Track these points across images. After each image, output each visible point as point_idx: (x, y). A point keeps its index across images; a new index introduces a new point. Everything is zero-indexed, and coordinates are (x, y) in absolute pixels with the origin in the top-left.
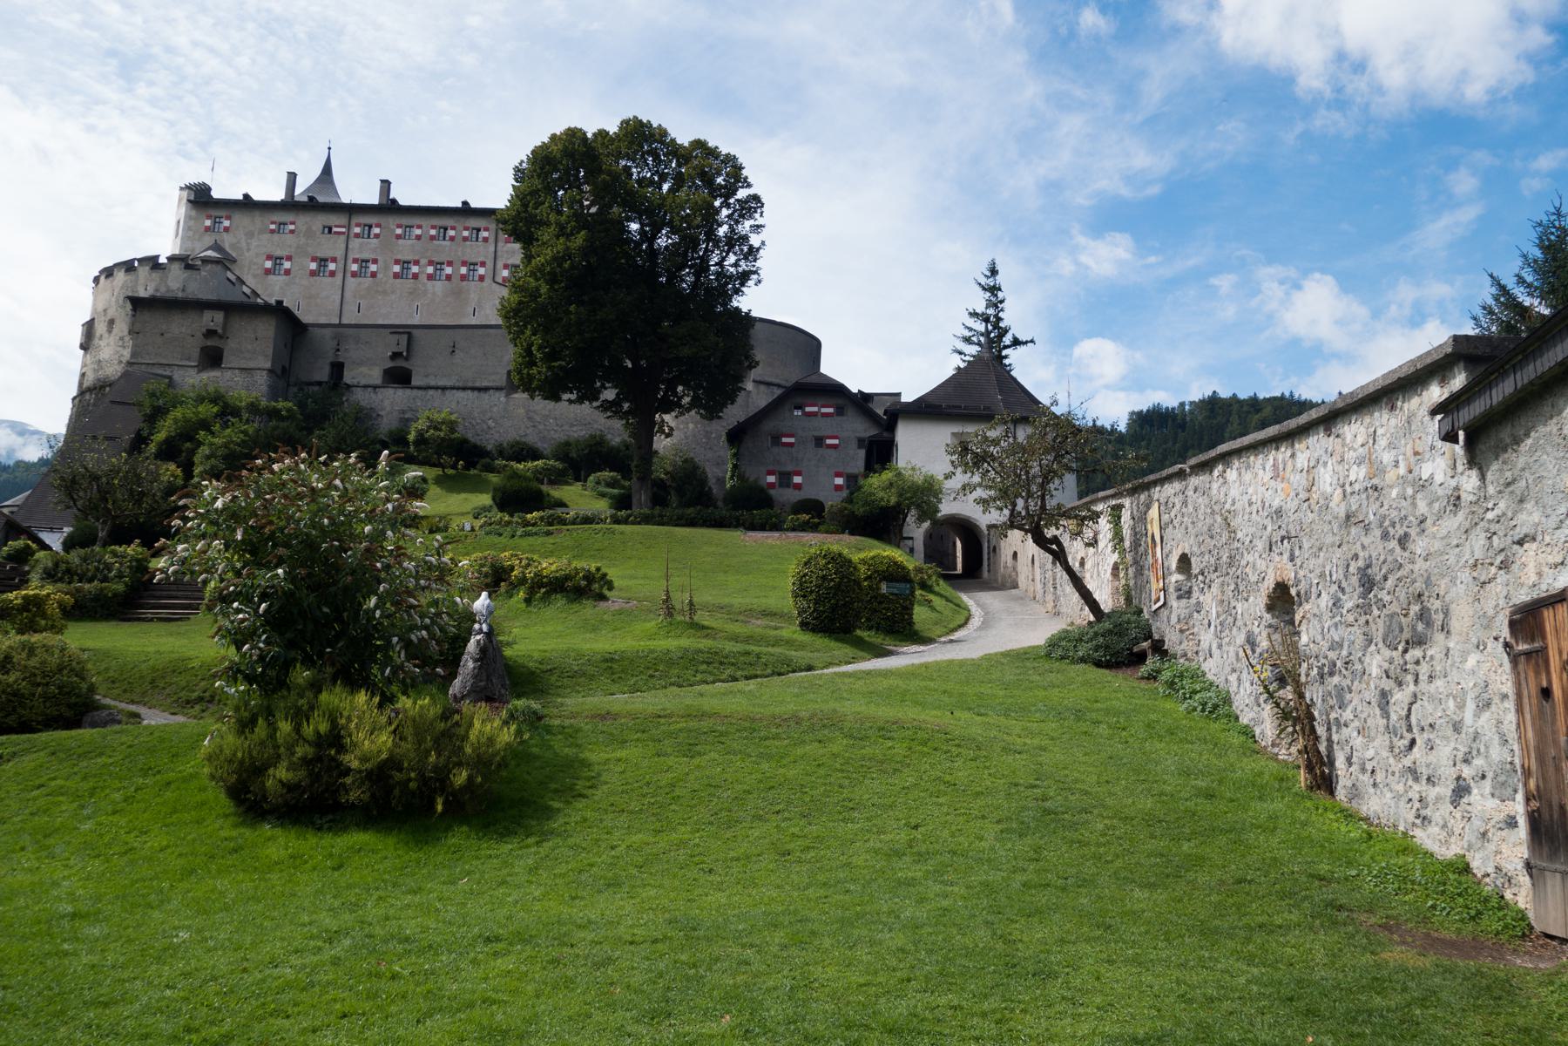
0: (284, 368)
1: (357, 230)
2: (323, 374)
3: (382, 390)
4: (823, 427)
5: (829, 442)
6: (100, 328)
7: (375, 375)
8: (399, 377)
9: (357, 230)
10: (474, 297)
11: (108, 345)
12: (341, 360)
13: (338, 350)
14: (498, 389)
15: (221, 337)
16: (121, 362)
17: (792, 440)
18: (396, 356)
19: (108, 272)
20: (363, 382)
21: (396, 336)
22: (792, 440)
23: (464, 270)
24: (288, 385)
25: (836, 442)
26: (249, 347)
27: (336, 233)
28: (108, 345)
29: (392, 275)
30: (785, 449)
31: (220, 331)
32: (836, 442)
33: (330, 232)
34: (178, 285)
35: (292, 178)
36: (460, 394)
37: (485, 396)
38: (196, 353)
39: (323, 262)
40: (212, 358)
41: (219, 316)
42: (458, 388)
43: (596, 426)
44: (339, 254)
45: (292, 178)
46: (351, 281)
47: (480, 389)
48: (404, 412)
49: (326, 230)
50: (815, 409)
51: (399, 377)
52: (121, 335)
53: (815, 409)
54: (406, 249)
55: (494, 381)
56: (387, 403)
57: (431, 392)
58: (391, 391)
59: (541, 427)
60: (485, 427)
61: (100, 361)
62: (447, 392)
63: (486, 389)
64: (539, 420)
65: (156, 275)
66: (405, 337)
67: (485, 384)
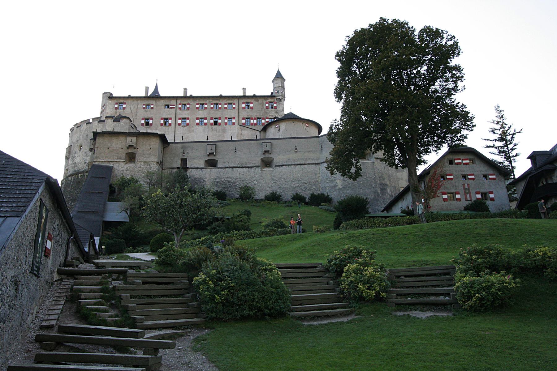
0: (161, 161)
1: (180, 106)
2: (178, 164)
3: (205, 169)
4: (466, 170)
5: (469, 177)
6: (76, 149)
7: (202, 164)
8: (212, 163)
9: (180, 106)
11: (79, 156)
12: (185, 157)
13: (184, 153)
14: (257, 167)
15: (135, 148)
16: (85, 163)
17: (452, 177)
18: (210, 154)
19: (78, 126)
20: (196, 166)
21: (211, 146)
22: (452, 177)
23: (226, 121)
24: (162, 169)
25: (473, 177)
26: (148, 152)
27: (172, 108)
28: (79, 156)
29: (195, 124)
30: (449, 181)
31: (135, 146)
32: (473, 177)
33: (168, 107)
34: (110, 129)
35: (147, 88)
36: (240, 170)
37: (252, 170)
38: (124, 156)
40: (131, 158)
41: (134, 139)
42: (239, 167)
43: (303, 181)
44: (173, 117)
45: (147, 88)
47: (248, 167)
48: (215, 179)
49: (167, 107)
50: (460, 161)
52: (85, 151)
53: (460, 161)
54: (201, 114)
55: (255, 164)
56: (207, 175)
57: (227, 169)
58: (209, 170)
59: (278, 183)
60: (253, 184)
61: (75, 163)
62: (234, 169)
63: (252, 167)
64: (277, 180)
65: (101, 125)
66: (214, 146)
67: (251, 165)
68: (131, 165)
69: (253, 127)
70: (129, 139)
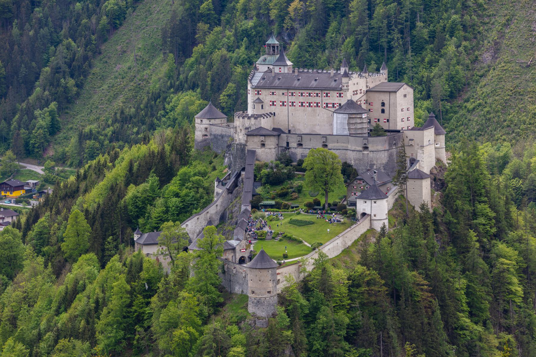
2: (285, 145)
8: (300, 145)
10: (318, 111)
38: (260, 145)
39: (283, 103)
41: (263, 137)
46: (290, 107)
51: (300, 145)
54: (302, 99)
65: (249, 120)
68: (263, 149)
69: (330, 109)
70: (261, 137)
